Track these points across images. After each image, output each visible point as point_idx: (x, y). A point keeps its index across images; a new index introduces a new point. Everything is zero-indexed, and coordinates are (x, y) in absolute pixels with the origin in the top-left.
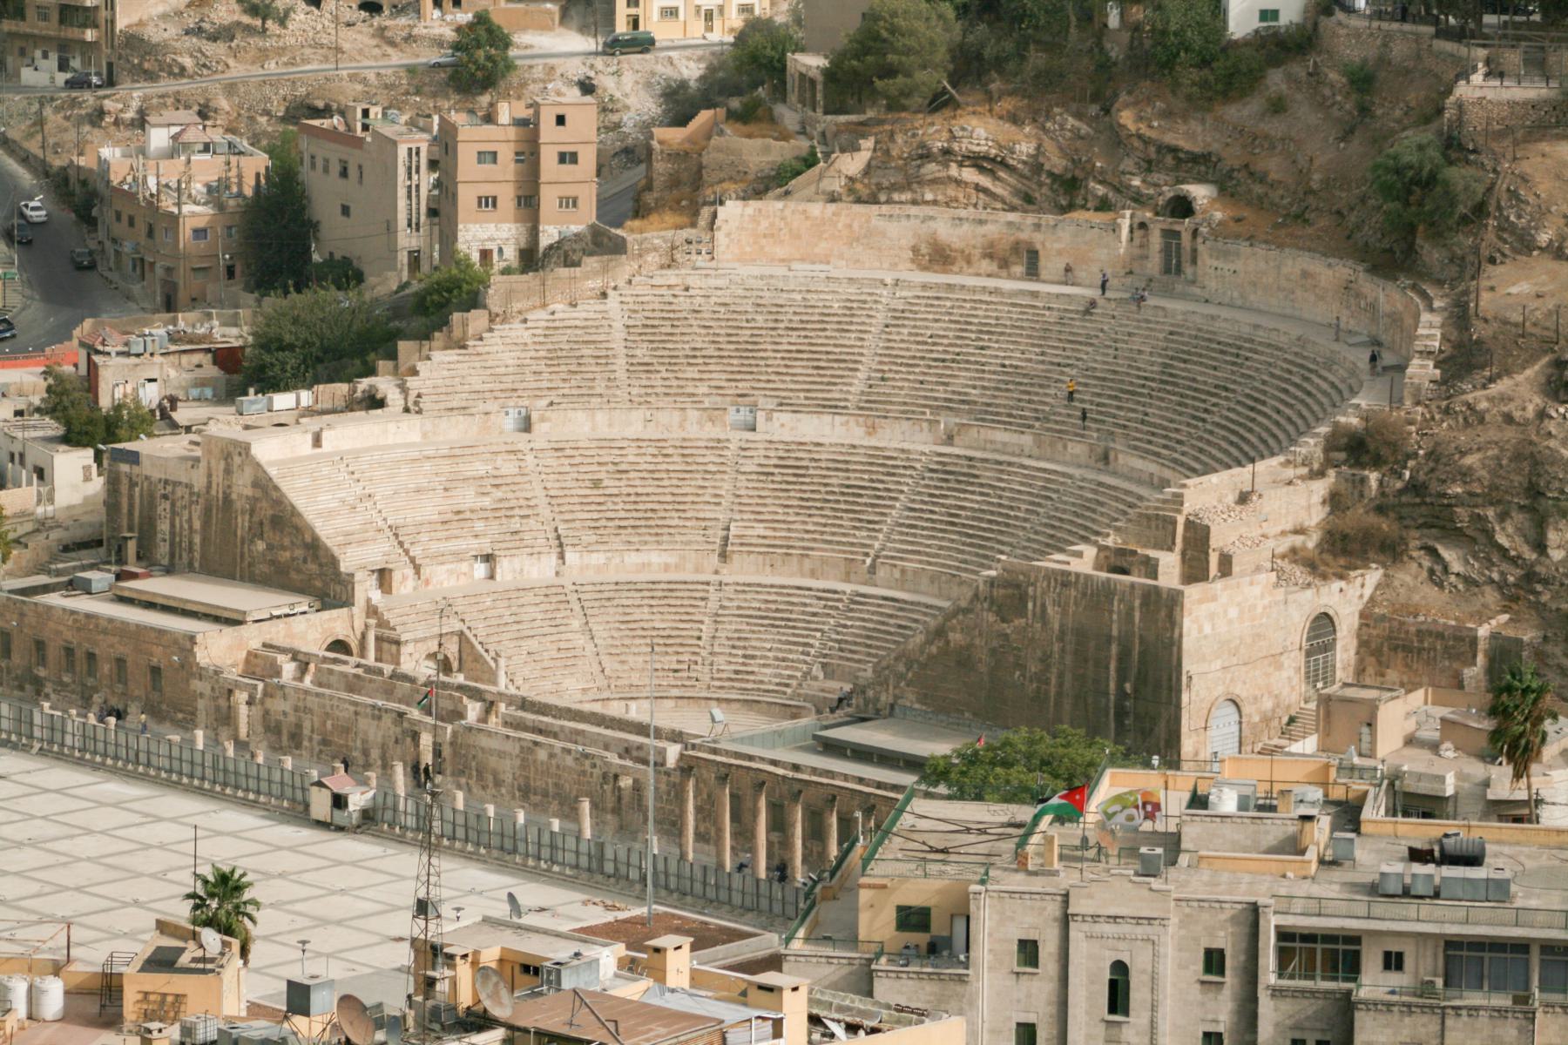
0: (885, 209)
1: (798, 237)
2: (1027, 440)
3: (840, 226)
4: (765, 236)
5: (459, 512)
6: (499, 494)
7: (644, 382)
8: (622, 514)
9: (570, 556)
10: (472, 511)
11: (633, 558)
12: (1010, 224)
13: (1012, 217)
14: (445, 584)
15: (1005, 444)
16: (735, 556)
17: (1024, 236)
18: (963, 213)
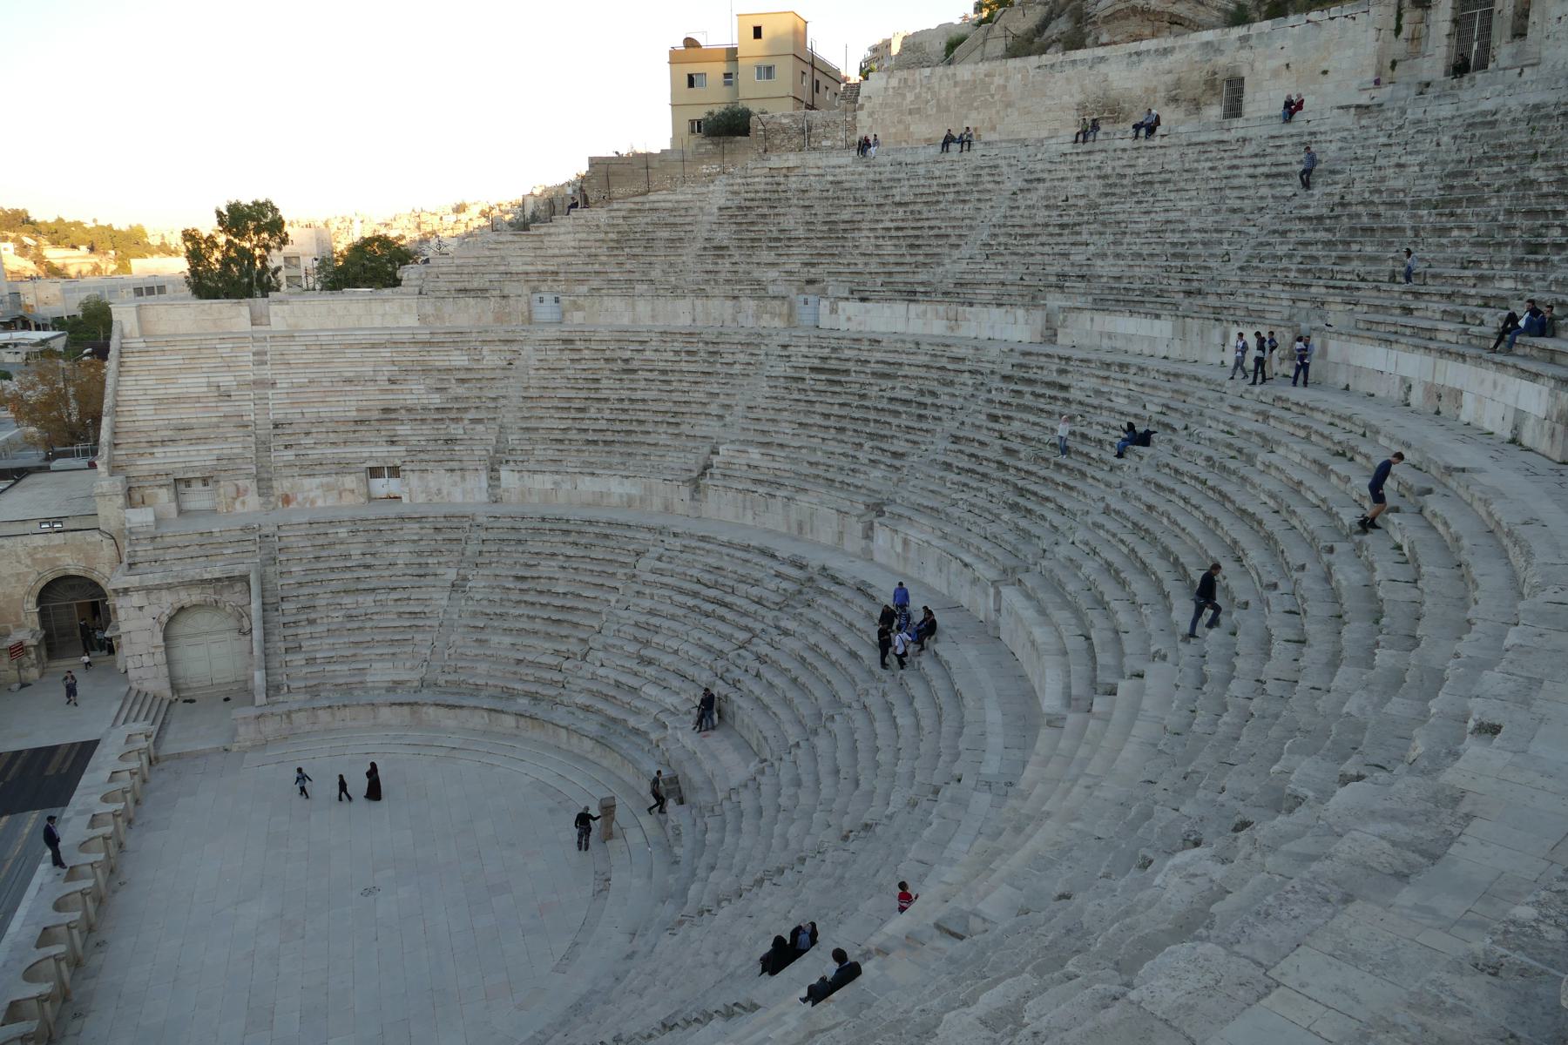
0: (1045, 59)
1: (947, 110)
2: (1163, 328)
3: (993, 88)
4: (910, 112)
5: (386, 410)
6: (460, 391)
7: (710, 267)
8: (602, 424)
9: (507, 477)
10: (409, 410)
11: (587, 485)
12: (1207, 43)
13: (1208, 35)
14: (320, 503)
15: (1129, 338)
16: (711, 492)
17: (1222, 61)
18: (1144, 45)
